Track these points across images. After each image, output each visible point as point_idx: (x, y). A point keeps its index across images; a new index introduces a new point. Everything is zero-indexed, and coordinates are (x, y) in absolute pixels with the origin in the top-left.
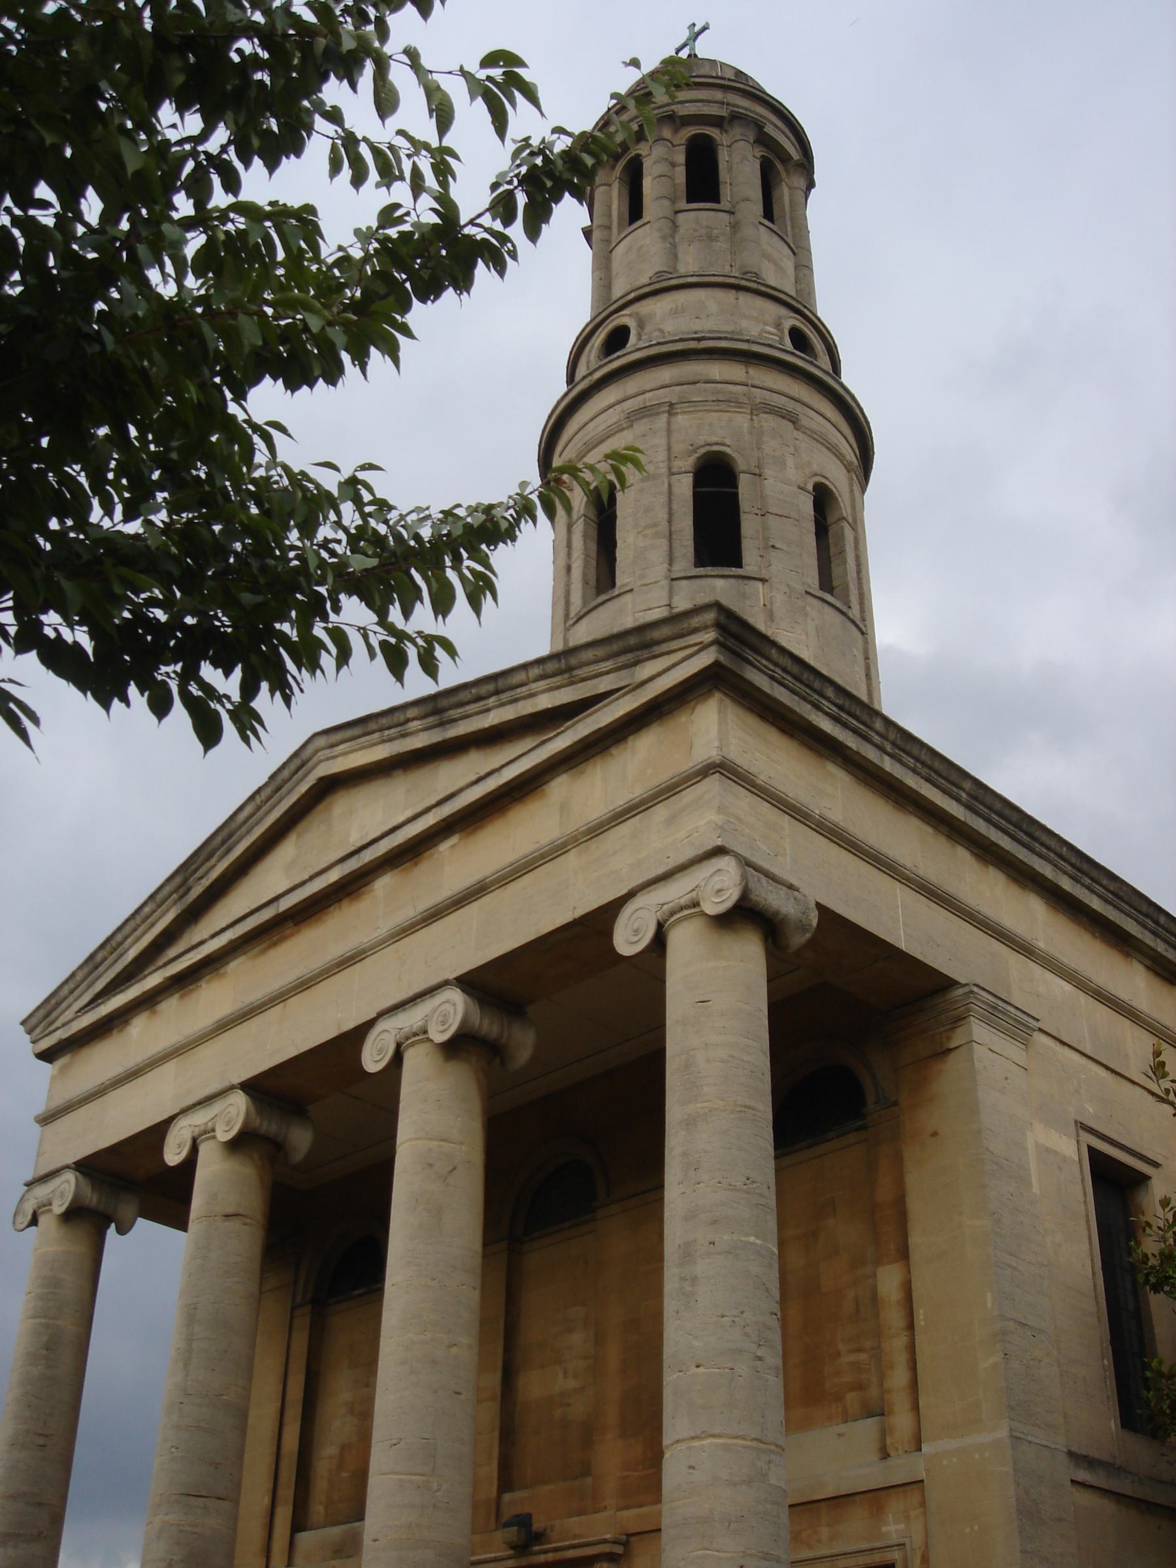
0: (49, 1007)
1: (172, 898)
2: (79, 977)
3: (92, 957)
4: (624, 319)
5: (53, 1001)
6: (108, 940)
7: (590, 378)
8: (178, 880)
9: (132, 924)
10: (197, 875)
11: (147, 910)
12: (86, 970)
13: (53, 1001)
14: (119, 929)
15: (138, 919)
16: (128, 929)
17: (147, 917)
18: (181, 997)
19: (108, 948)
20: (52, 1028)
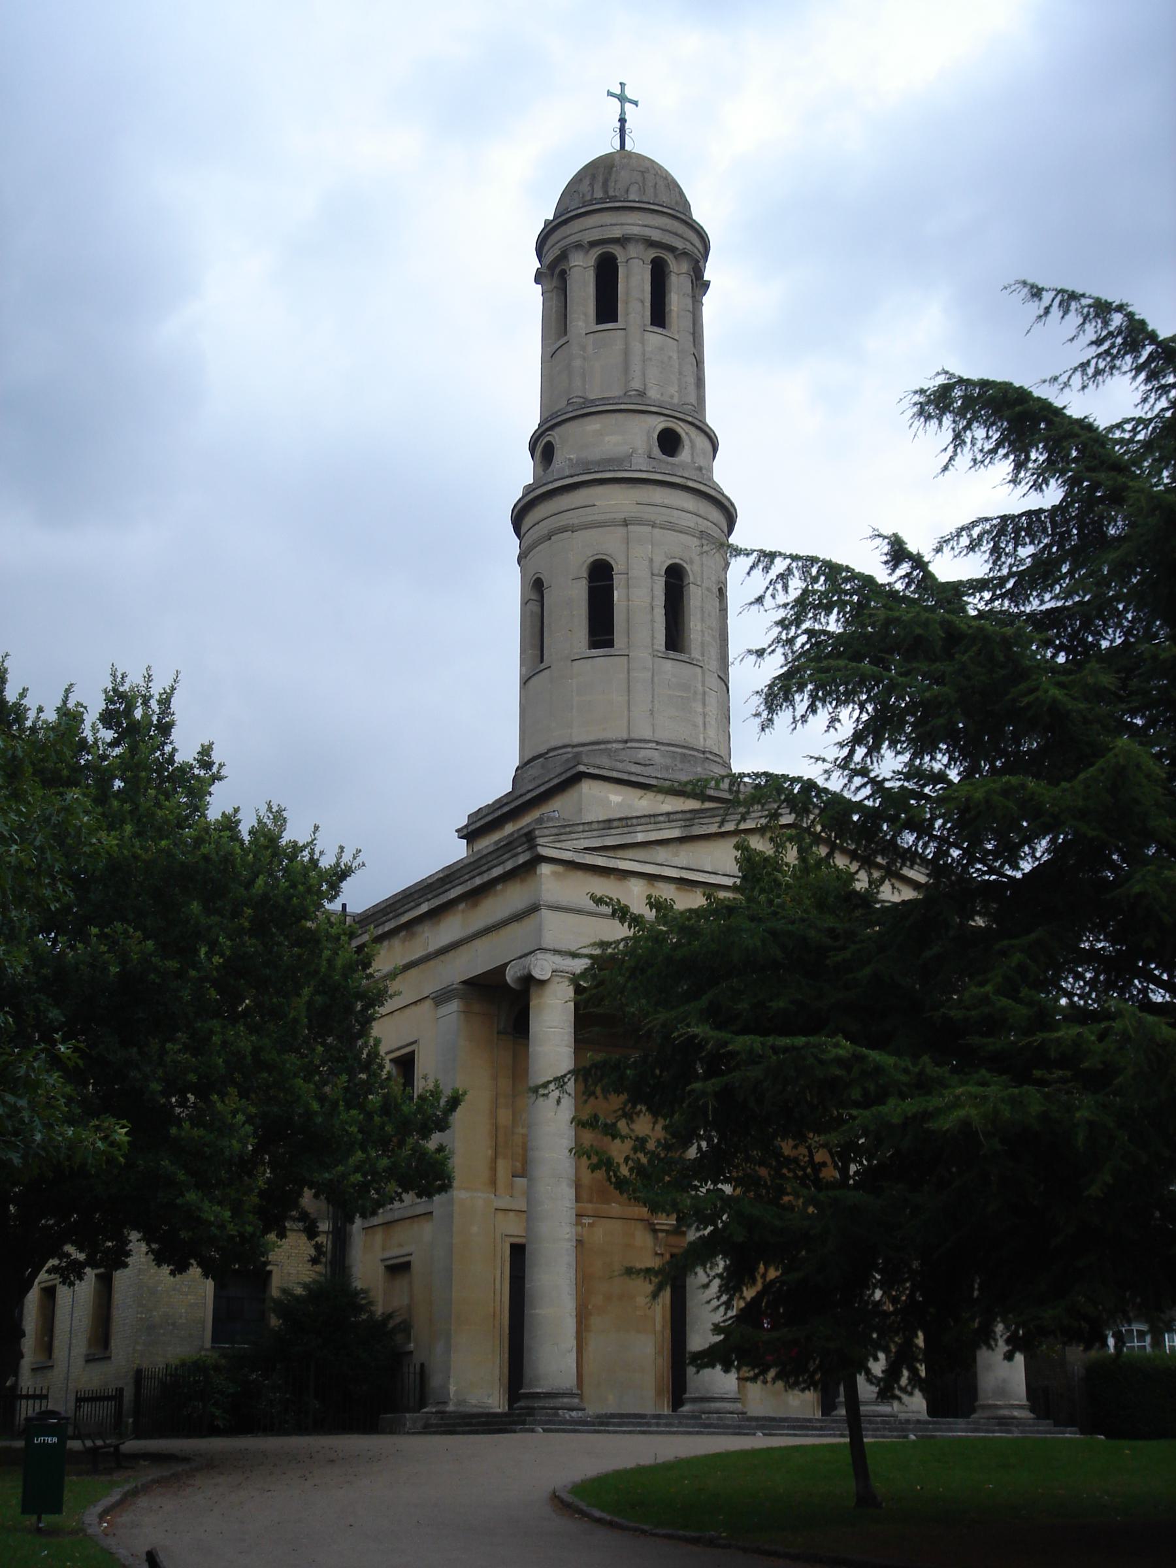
0: (563, 831)
1: (680, 822)
2: (595, 826)
3: (610, 821)
4: (681, 429)
5: (568, 829)
6: (627, 818)
7: (685, 480)
8: (688, 816)
9: (647, 820)
10: (702, 821)
11: (661, 818)
12: (601, 826)
13: (568, 829)
14: (637, 817)
15: (652, 820)
16: (643, 820)
17: (659, 823)
18: (678, 889)
19: (624, 823)
20: (558, 845)
